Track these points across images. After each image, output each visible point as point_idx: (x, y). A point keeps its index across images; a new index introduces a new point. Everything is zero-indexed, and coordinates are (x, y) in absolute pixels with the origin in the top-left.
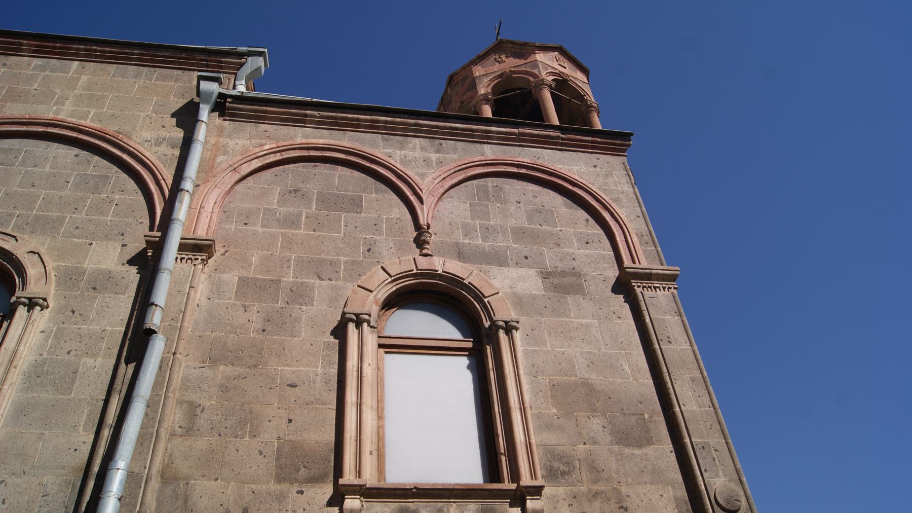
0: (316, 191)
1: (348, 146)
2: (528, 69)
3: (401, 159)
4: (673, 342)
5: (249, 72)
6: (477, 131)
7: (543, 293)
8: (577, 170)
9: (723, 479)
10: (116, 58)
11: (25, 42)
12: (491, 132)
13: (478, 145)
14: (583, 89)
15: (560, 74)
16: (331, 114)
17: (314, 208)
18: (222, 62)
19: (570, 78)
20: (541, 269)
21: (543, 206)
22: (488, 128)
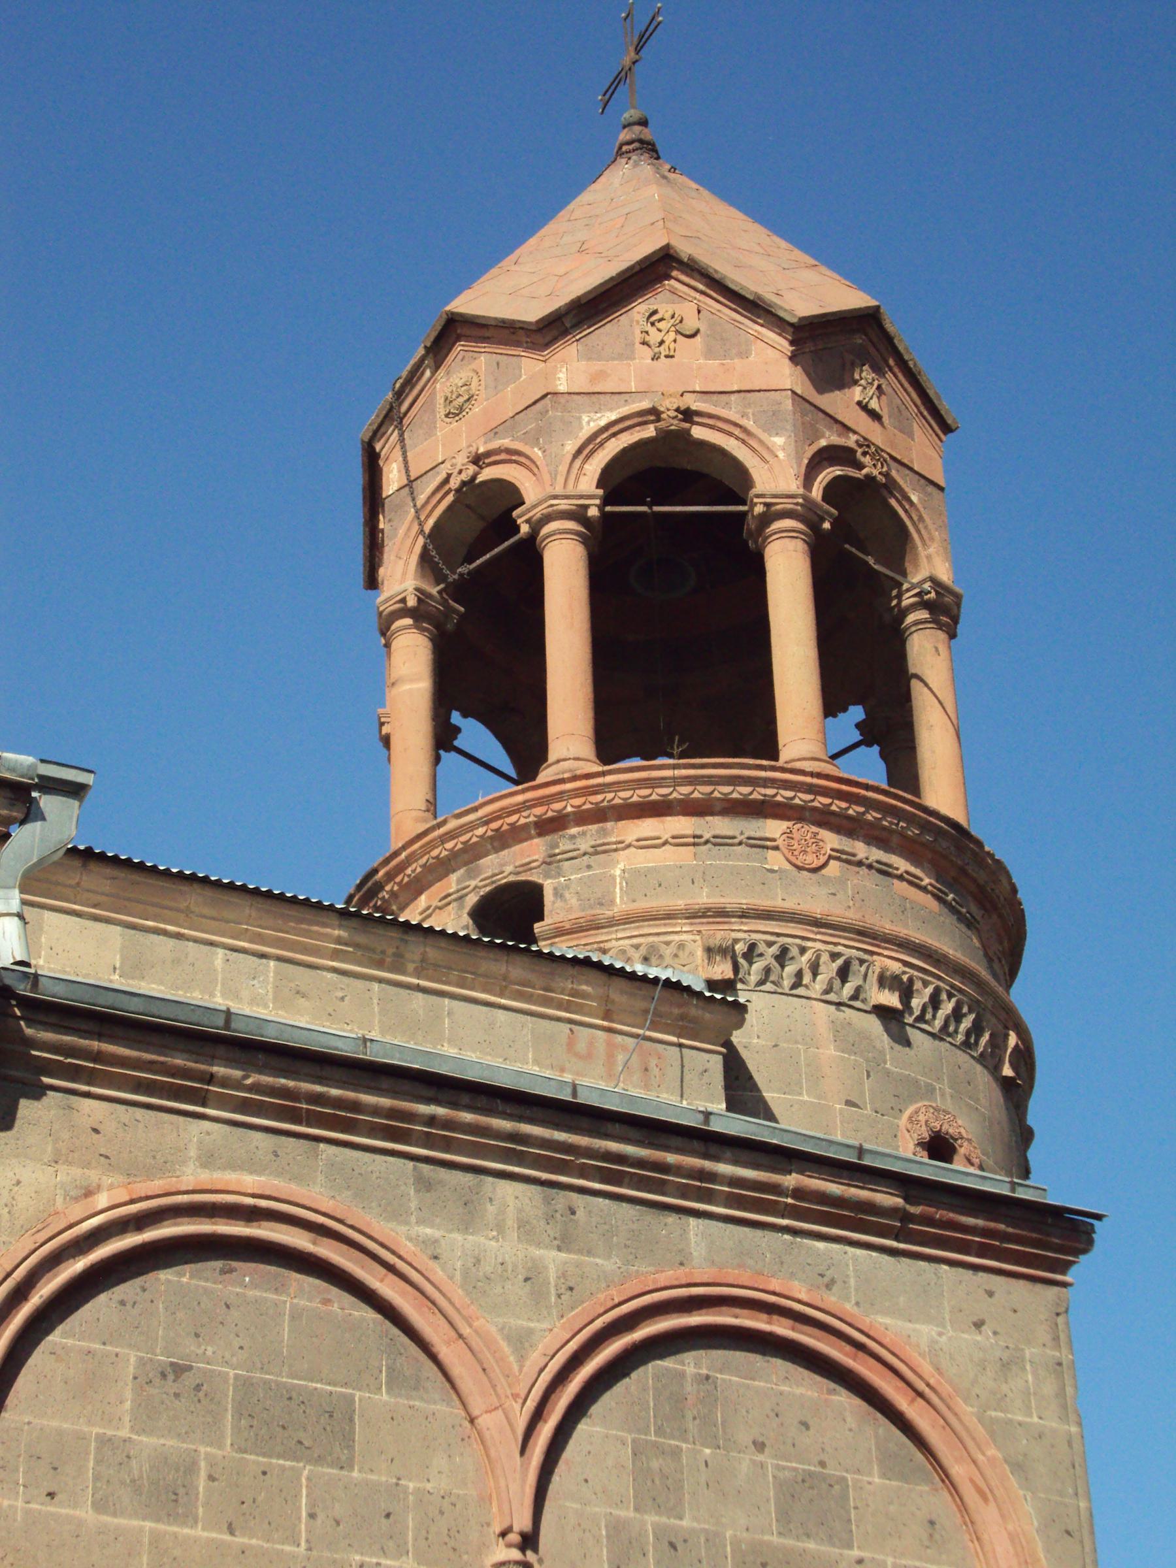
0: (232, 1373)
1: (326, 1205)
3: (466, 1273)
5: (35, 860)
6: (677, 1170)
12: (712, 1177)
13: (672, 1219)
14: (921, 518)
16: (283, 1081)
17: (229, 1442)
21: (822, 1464)
22: (707, 1165)
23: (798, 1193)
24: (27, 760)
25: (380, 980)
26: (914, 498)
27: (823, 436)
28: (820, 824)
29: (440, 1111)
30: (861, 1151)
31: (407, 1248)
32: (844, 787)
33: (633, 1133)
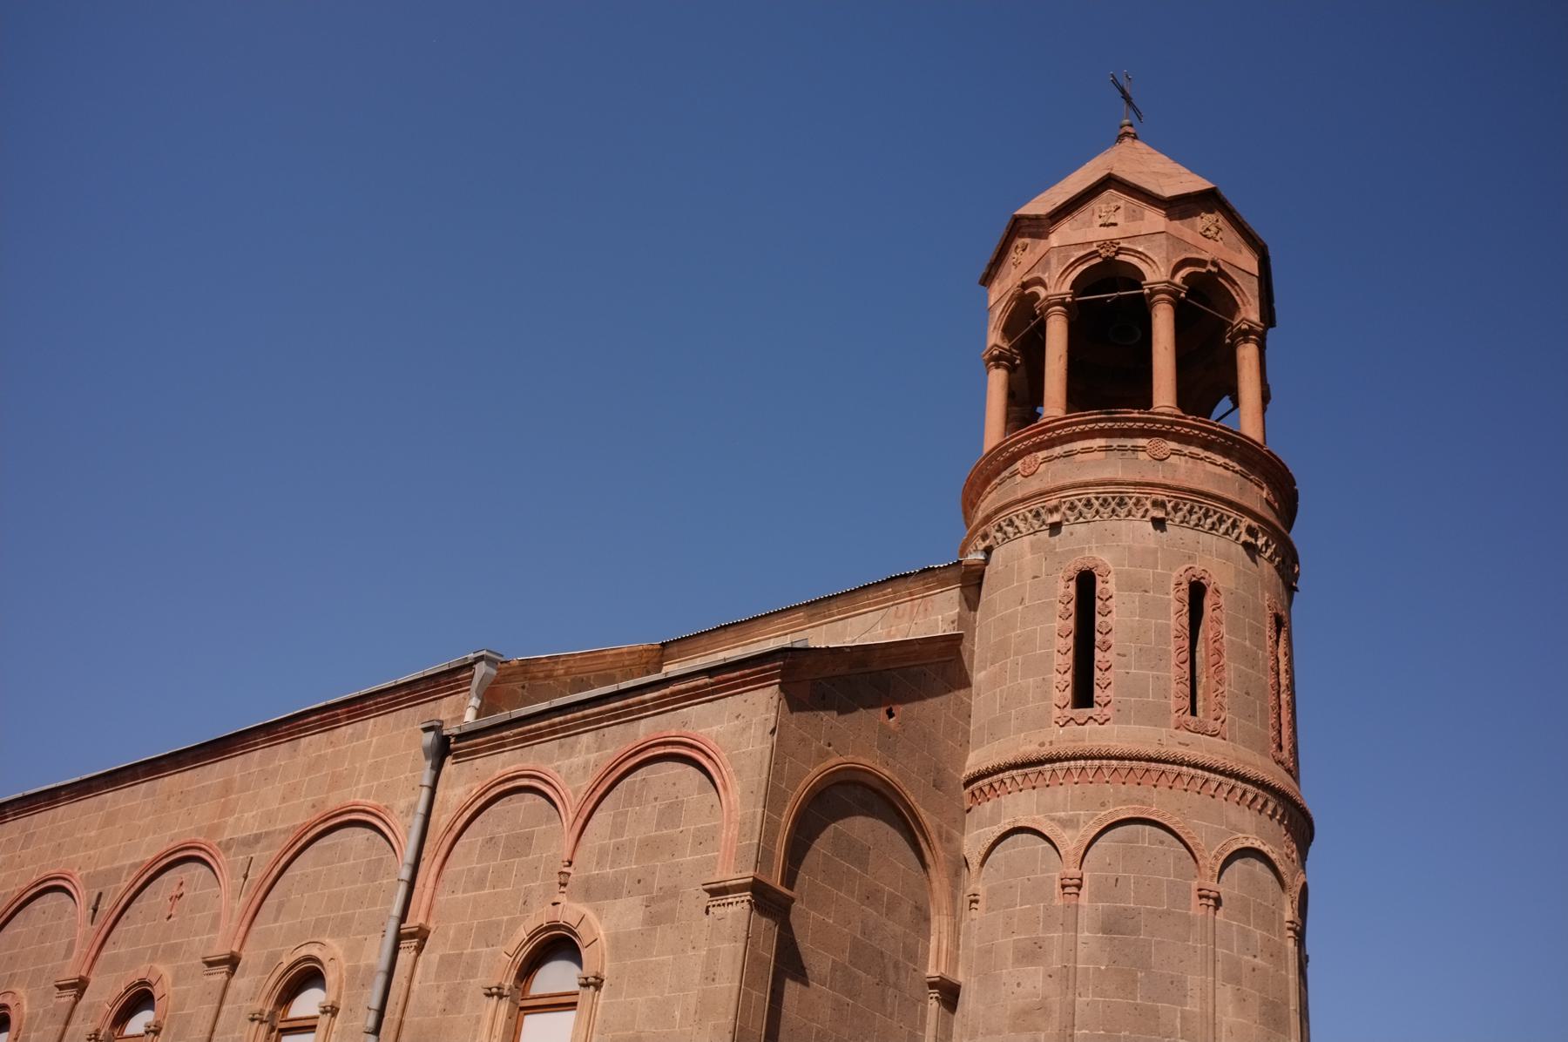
2: (1040, 275)
4: (717, 980)
7: (640, 928)
8: (718, 731)
10: (391, 706)
11: (339, 711)
14: (1146, 256)
15: (1096, 251)
18: (458, 680)
19: (1123, 245)
23: (673, 694)
25: (826, 623)
26: (1140, 250)
27: (1072, 256)
28: (1039, 450)
29: (561, 718)
30: (725, 659)
31: (551, 772)
32: (1040, 429)
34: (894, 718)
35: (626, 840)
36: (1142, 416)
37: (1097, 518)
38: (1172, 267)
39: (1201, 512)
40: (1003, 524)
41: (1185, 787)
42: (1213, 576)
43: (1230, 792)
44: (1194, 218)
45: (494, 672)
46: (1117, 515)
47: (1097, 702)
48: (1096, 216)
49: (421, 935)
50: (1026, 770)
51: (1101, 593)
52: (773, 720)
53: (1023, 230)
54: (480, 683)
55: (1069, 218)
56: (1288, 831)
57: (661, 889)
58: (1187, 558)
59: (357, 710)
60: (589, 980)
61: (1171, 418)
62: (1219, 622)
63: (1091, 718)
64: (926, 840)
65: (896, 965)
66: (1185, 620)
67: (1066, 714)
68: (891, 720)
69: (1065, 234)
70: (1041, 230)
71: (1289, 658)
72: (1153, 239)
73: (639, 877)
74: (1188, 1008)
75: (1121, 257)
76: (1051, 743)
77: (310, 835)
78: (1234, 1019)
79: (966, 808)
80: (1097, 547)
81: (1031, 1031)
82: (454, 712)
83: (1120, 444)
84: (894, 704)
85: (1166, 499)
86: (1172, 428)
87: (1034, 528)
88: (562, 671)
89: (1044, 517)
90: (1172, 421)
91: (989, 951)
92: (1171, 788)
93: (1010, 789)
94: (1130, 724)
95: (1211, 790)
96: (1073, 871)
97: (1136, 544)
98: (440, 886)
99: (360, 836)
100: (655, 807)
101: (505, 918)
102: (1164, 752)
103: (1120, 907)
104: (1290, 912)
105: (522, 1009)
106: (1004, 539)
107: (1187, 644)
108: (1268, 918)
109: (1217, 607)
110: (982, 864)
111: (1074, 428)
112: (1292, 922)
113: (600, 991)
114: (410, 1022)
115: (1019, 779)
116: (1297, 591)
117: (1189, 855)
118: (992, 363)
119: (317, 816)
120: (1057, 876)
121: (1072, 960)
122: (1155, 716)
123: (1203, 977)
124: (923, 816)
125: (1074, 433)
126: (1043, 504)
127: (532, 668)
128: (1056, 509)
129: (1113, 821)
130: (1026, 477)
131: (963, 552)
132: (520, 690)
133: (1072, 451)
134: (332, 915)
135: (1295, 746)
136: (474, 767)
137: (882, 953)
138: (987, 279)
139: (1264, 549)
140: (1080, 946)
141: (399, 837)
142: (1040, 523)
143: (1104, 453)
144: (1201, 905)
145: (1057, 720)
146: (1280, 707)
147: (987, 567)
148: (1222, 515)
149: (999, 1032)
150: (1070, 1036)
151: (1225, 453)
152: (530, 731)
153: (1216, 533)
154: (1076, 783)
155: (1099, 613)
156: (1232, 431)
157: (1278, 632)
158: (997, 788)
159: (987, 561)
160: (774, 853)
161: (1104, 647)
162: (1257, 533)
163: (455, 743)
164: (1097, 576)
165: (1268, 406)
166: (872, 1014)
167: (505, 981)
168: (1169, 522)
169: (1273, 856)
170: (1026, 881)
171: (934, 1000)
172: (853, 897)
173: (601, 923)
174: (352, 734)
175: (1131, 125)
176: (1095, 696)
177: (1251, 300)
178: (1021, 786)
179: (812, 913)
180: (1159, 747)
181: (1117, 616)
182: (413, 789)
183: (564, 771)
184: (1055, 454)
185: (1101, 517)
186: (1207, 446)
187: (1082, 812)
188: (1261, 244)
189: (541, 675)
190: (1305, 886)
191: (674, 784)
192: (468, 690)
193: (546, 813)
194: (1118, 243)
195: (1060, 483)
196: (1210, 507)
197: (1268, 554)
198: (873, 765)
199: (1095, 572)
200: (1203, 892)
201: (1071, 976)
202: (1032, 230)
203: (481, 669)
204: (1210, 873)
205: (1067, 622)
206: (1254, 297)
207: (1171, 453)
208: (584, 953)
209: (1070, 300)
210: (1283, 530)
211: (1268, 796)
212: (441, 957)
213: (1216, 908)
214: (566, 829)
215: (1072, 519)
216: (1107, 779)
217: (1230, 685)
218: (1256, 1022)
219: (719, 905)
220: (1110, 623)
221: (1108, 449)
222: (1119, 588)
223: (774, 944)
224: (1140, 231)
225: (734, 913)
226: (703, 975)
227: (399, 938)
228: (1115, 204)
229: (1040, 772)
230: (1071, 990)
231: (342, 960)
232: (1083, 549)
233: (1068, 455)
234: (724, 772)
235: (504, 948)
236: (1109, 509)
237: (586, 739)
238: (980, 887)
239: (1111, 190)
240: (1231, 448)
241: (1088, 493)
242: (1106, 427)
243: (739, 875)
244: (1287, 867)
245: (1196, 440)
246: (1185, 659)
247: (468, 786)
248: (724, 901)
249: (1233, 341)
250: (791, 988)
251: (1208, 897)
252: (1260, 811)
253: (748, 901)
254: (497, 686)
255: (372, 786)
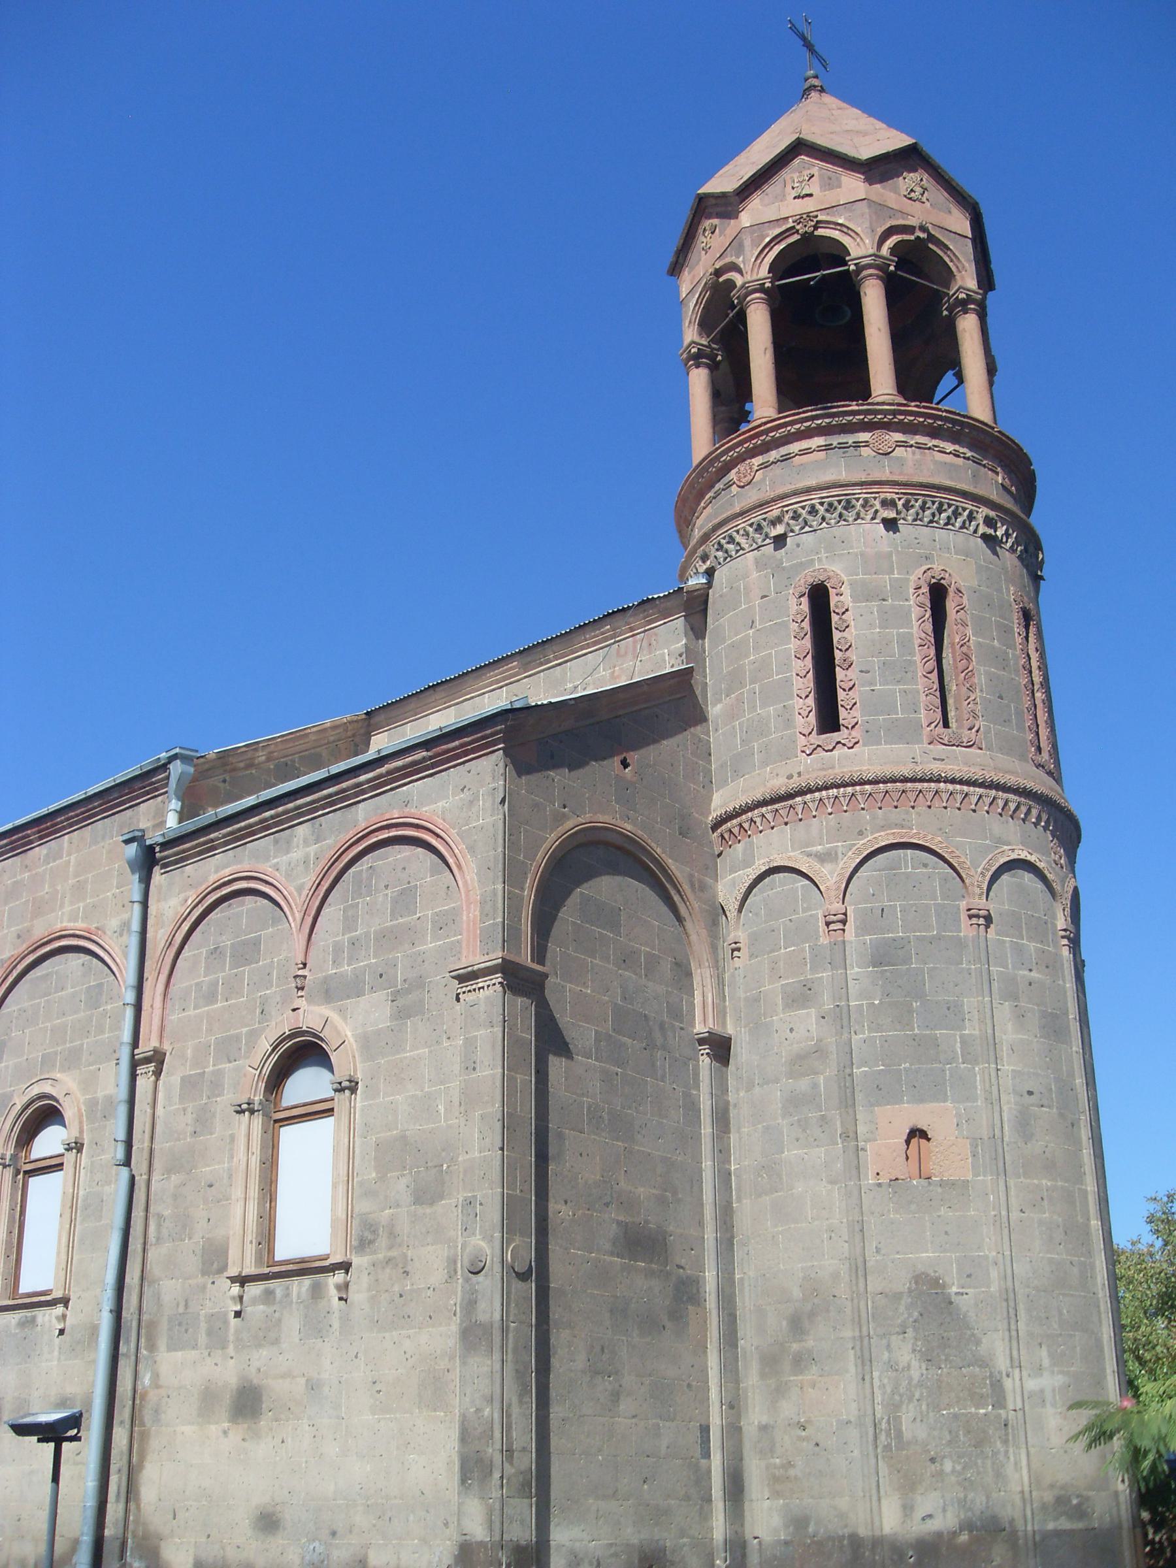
1: (247, 867)
2: (733, 259)
7: (389, 1024)
8: (443, 807)
9: (478, 1237)
11: (29, 832)
15: (793, 227)
16: (229, 829)
19: (820, 218)
20: (392, 988)
23: (389, 773)
24: (164, 754)
26: (840, 221)
27: (768, 236)
28: (753, 457)
29: (272, 812)
30: (441, 729)
33: (328, 783)
34: (629, 768)
35: (361, 934)
36: (861, 408)
37: (824, 525)
38: (877, 238)
39: (935, 507)
40: (723, 542)
41: (944, 804)
42: (953, 574)
43: (991, 804)
44: (895, 179)
45: (192, 770)
46: (845, 520)
47: (843, 725)
48: (789, 188)
49: (157, 1059)
50: (776, 806)
51: (837, 607)
52: (501, 789)
53: (710, 210)
54: (177, 785)
55: (759, 192)
56: (1053, 836)
57: (405, 980)
58: (924, 559)
59: (47, 828)
60: (343, 1085)
61: (893, 407)
62: (965, 625)
63: (839, 743)
64: (679, 892)
65: (662, 1027)
66: (929, 627)
67: (812, 741)
68: (627, 770)
69: (754, 211)
70: (730, 209)
71: (1040, 653)
72: (854, 208)
73: (380, 970)
74: (967, 1032)
75: (821, 232)
76: (799, 774)
77: (20, 968)
78: (1014, 1036)
79: (717, 853)
80: (827, 557)
81: (808, 1075)
82: (154, 817)
83: (841, 441)
84: (627, 752)
85: (895, 496)
86: (895, 417)
87: (757, 543)
88: (264, 758)
89: (766, 529)
90: (895, 410)
91: (757, 1000)
92: (930, 807)
93: (761, 828)
94: (881, 744)
95: (971, 804)
96: (837, 907)
97: (868, 550)
98: (169, 1004)
99: (74, 963)
100: (387, 895)
101: (245, 1030)
102: (919, 770)
103: (889, 938)
104: (1063, 920)
105: (276, 1121)
106: (725, 559)
107: (932, 652)
108: (1041, 929)
109: (961, 609)
110: (740, 910)
111: (789, 428)
112: (1065, 930)
113: (356, 1094)
114: (161, 1149)
115: (769, 816)
116: (1044, 580)
117: (955, 875)
118: (691, 363)
119: (25, 946)
120: (820, 916)
121: (844, 998)
122: (904, 732)
123: (980, 998)
124: (673, 867)
125: (790, 434)
126: (764, 516)
127: (230, 759)
128: (778, 520)
129: (873, 849)
130: (743, 487)
131: (683, 577)
132: (221, 785)
133: (790, 454)
134: (59, 1049)
135: (1055, 746)
136: (186, 875)
137: (645, 1016)
138: (676, 269)
139: (1004, 540)
140: (851, 983)
141: (118, 961)
142: (763, 536)
143: (825, 452)
144: (971, 925)
145: (803, 749)
146: (1035, 706)
147: (710, 591)
148: (957, 507)
149: (777, 1081)
150: (849, 1075)
151: (954, 438)
152: (240, 830)
153: (953, 528)
154: (830, 814)
155: (837, 629)
156: (959, 415)
157: (1027, 627)
158: (747, 828)
159: (709, 584)
160: (520, 929)
161: (846, 666)
162: (996, 523)
163: (160, 852)
164: (830, 589)
165: (995, 378)
166: (642, 1079)
167: (254, 1096)
168: (902, 521)
169: (1041, 865)
170: (788, 922)
171: (705, 1056)
172: (609, 962)
173: (346, 1023)
174: (47, 854)
175: (816, 77)
176: (841, 719)
177: (967, 265)
178: (772, 824)
179: (568, 985)
180: (912, 766)
181: (856, 630)
182: (123, 906)
183: (283, 868)
184: (771, 460)
185: (827, 524)
186: (934, 433)
187: (839, 844)
188: (971, 201)
189: (242, 765)
190: (1076, 893)
191: (404, 869)
192: (166, 792)
193: (270, 915)
194: (817, 216)
195: (781, 490)
196: (943, 500)
197: (1009, 545)
198: (613, 822)
199: (828, 585)
200: (972, 912)
201: (845, 1016)
202: (719, 209)
203: (176, 768)
204: (977, 891)
205: (803, 642)
206: (968, 261)
207: (897, 446)
208: (333, 1058)
209: (770, 285)
210: (1023, 516)
211: (1031, 803)
212: (183, 1079)
213: (987, 927)
214: (294, 929)
215: (797, 528)
216: (862, 806)
217: (981, 691)
218: (1036, 1036)
219: (470, 991)
220: (849, 638)
221: (828, 448)
222: (855, 599)
223: (533, 1024)
224: (839, 201)
225: (487, 998)
226: (463, 1065)
227: (134, 1065)
228: (809, 172)
229: (791, 806)
230: (846, 1029)
231: (79, 1095)
232: (813, 560)
233: (786, 458)
234: (456, 851)
235: (248, 1062)
236: (836, 515)
237: (302, 831)
238: (740, 934)
239: (802, 157)
240: (959, 433)
241: (811, 499)
242: (824, 424)
243: (486, 958)
244: (1057, 874)
245: (921, 428)
246: (932, 668)
247: (182, 896)
248: (474, 987)
249: (951, 313)
250: (557, 1065)
251: (978, 916)
252: (1024, 820)
253: (499, 983)
254: (197, 783)
255: (79, 908)
